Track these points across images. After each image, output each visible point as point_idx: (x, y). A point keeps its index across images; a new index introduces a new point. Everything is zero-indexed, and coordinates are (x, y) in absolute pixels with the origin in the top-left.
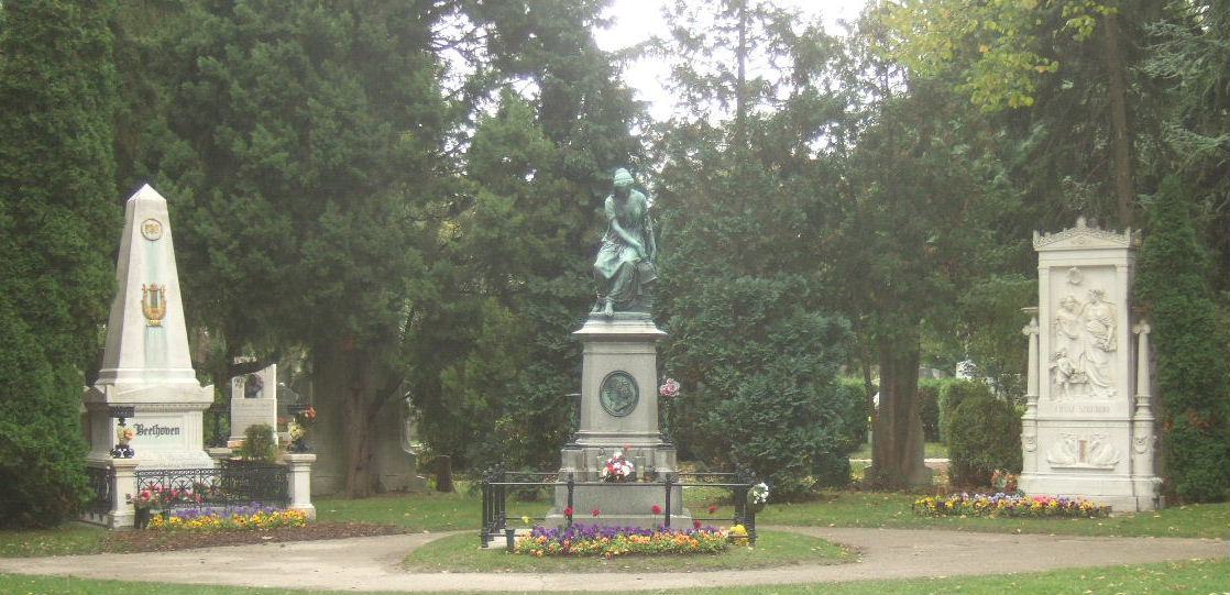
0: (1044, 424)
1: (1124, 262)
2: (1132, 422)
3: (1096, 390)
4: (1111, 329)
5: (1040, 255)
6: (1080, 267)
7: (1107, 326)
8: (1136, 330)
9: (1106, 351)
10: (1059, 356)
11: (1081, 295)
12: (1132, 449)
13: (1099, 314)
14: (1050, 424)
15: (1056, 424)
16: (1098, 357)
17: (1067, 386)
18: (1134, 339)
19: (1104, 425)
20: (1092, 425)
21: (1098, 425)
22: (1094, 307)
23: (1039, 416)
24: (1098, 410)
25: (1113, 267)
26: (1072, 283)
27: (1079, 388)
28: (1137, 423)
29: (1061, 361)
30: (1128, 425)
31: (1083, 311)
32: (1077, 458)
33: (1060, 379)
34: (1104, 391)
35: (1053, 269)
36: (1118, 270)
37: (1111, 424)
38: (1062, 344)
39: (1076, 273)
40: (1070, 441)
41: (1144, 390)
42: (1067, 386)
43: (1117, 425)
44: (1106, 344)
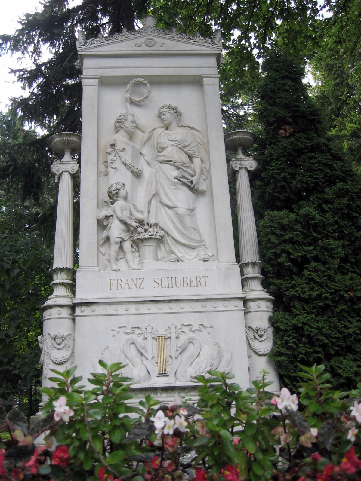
0: (87, 310)
1: (214, 71)
2: (245, 301)
3: (180, 252)
4: (197, 161)
5: (87, 63)
6: (142, 77)
7: (190, 157)
8: (236, 165)
9: (193, 189)
10: (113, 196)
11: (145, 117)
12: (249, 345)
13: (179, 137)
14: (98, 310)
15: (111, 309)
16: (181, 197)
17: (127, 245)
18: (233, 176)
19: (198, 306)
20: (176, 307)
21: (187, 307)
22: (166, 131)
23: (81, 295)
24: (187, 282)
25: (197, 82)
26: (132, 102)
27: (148, 249)
28: (253, 305)
29: (120, 203)
30: (241, 303)
31: (149, 139)
32: (155, 370)
33: (116, 230)
34: (194, 253)
35: (106, 82)
36: (205, 81)
37: (210, 306)
38: (120, 176)
39: (137, 87)
40: (140, 340)
41: (251, 254)
42: (127, 245)
43: (220, 306)
44: (194, 179)
